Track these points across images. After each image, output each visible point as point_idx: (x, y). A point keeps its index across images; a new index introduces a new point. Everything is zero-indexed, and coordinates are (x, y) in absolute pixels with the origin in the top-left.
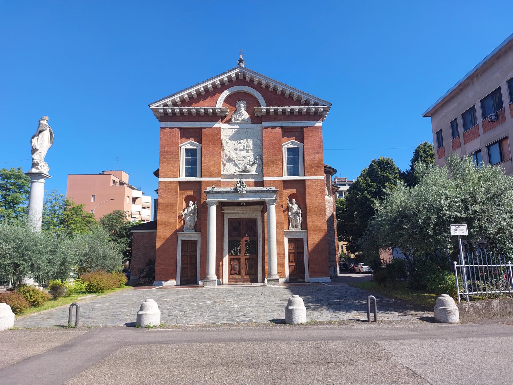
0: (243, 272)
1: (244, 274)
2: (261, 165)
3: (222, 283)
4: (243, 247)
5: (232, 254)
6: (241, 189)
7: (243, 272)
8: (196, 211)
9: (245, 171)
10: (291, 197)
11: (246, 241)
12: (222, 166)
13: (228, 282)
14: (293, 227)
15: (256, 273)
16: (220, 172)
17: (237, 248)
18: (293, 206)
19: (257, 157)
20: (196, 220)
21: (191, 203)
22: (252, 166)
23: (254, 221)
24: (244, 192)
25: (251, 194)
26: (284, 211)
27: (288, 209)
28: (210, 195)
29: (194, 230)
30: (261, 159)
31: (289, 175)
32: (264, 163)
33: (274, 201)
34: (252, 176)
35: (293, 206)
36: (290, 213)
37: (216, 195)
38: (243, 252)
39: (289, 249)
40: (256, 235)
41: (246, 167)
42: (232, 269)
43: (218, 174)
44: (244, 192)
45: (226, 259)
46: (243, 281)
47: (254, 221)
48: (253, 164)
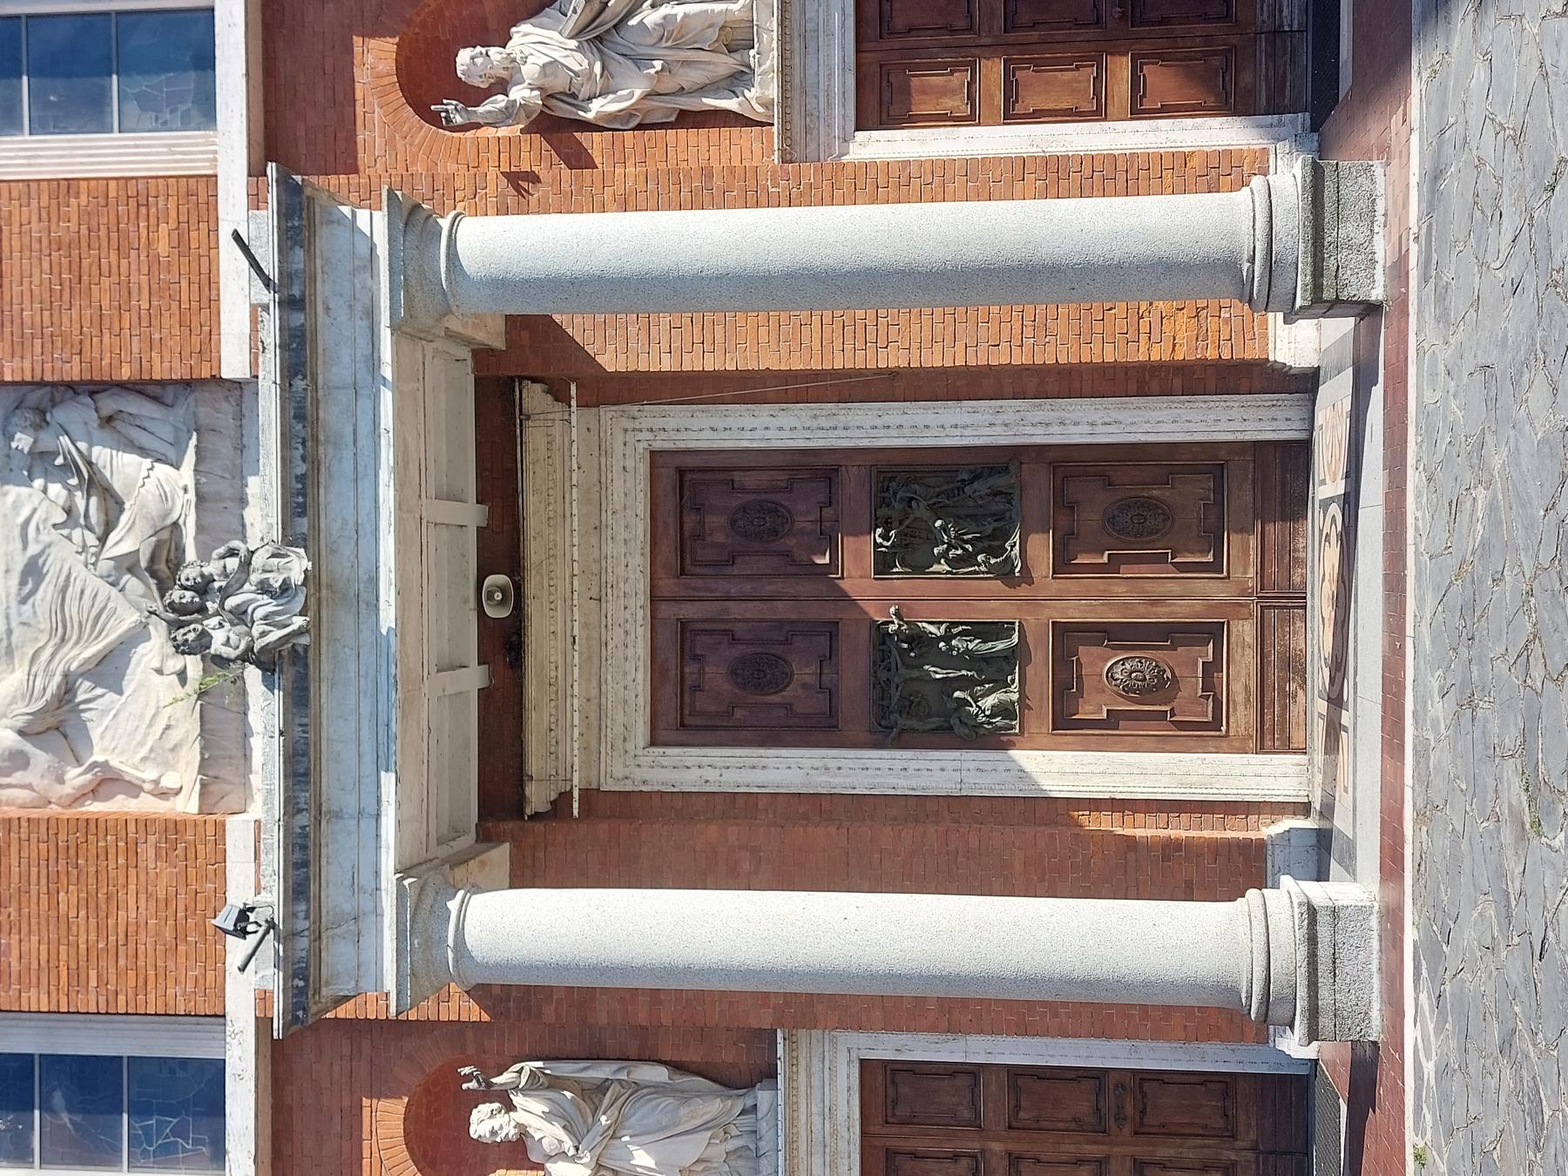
0: (1182, 595)
1: (1214, 590)
2: (109, 404)
3: (1304, 809)
4: (935, 599)
5: (1004, 710)
6: (266, 605)
7: (1182, 595)
8: (565, 1069)
9: (162, 564)
10: (428, 85)
11: (883, 565)
12: (117, 805)
13: (1287, 748)
14: (739, 79)
15: (1210, 462)
16: (174, 827)
17: (946, 660)
18: (530, 71)
19: (23, 441)
20: (660, 1074)
21: (484, 1122)
22: (113, 504)
23: (684, 483)
24: (297, 566)
25: (335, 500)
26: (579, 160)
27: (557, 125)
28: (338, 955)
29: (763, 1096)
30: (43, 399)
31: (205, 111)
32: (73, 372)
33: (413, 221)
34: (219, 501)
35: (530, 71)
36: (597, 108)
37: (334, 895)
38: (985, 598)
39: (971, 119)
40: (819, 470)
41: (128, 564)
42: (1160, 712)
43: (194, 846)
44: (297, 566)
45: (1055, 769)
46: (1282, 600)
47: (684, 483)
48: (96, 484)
